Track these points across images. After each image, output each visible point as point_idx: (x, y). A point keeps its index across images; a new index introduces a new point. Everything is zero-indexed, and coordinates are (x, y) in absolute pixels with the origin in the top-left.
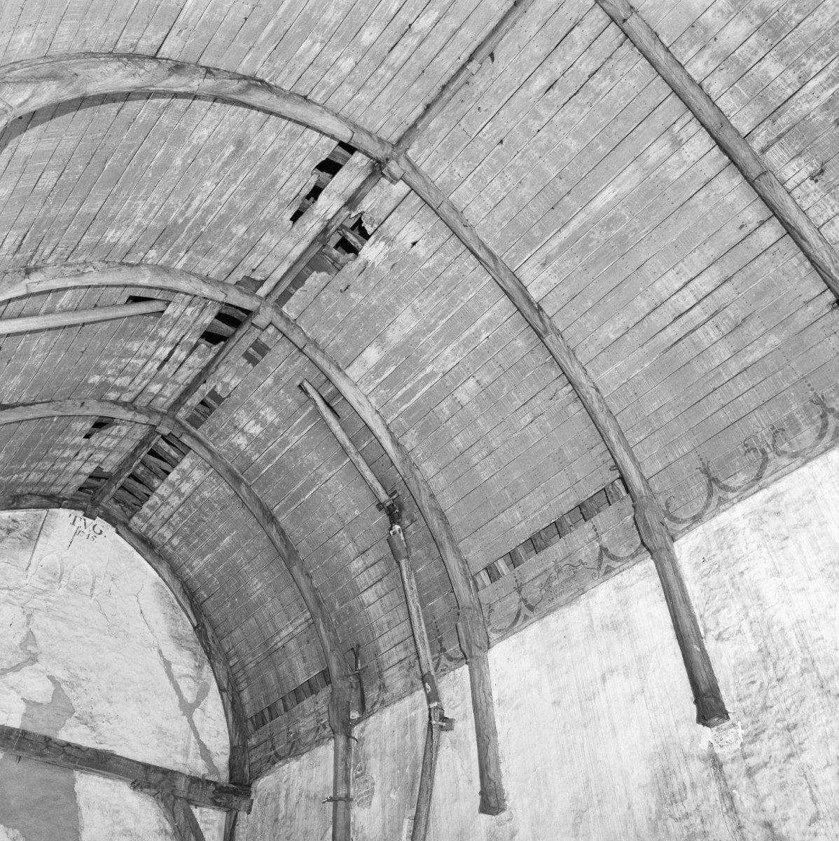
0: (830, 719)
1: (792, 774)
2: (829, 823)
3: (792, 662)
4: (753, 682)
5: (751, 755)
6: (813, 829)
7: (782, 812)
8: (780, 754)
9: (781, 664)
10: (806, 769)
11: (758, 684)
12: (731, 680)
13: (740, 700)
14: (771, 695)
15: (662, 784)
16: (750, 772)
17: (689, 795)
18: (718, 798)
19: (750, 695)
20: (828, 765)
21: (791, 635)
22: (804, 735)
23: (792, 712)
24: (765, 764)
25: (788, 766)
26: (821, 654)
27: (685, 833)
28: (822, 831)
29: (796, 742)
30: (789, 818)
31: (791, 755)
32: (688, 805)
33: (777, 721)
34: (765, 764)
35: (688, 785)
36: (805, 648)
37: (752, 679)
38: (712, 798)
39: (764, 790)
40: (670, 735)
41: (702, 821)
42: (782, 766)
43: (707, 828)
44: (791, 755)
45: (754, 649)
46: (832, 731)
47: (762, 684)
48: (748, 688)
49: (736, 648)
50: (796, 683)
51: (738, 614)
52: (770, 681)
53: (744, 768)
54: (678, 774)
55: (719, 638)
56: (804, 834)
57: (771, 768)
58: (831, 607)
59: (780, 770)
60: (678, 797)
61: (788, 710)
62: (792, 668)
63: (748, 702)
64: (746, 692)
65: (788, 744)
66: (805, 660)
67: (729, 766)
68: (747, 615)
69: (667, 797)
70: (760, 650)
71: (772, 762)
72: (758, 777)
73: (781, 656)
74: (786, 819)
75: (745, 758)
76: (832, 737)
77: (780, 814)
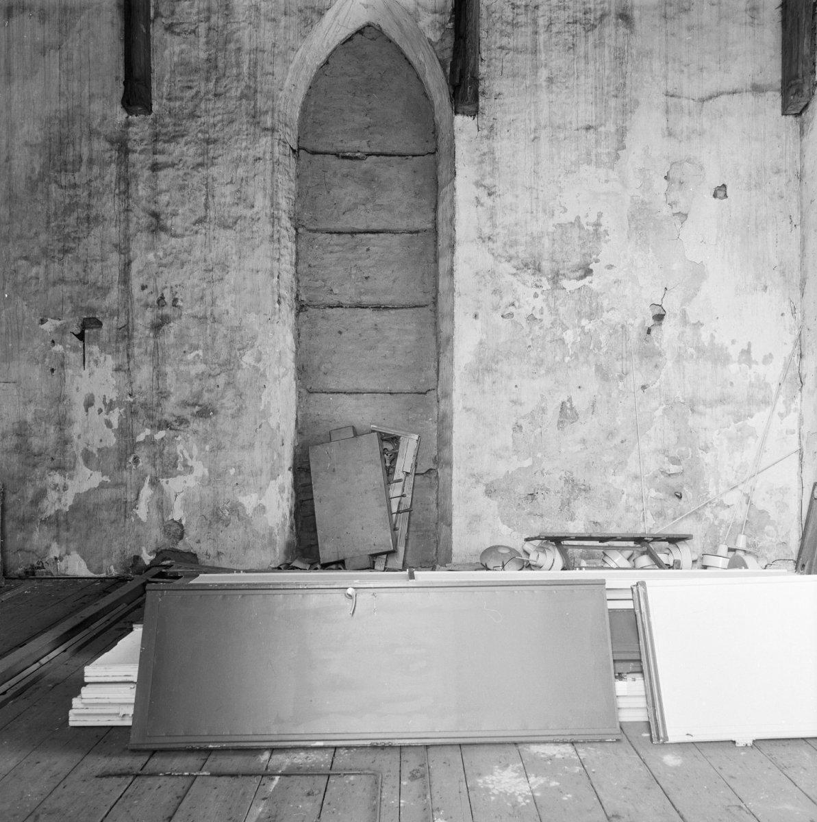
0: (249, 146)
1: (196, 179)
2: (212, 227)
3: (235, 84)
4: (190, 88)
5: (162, 152)
6: (195, 228)
7: (173, 208)
8: (191, 161)
9: (224, 82)
10: (210, 180)
11: (194, 91)
12: (167, 77)
13: (170, 99)
14: (203, 106)
15: (54, 148)
16: (155, 167)
17: (83, 169)
18: (114, 179)
19: (182, 99)
20: (231, 182)
21: (245, 58)
22: (220, 152)
23: (217, 129)
24: (173, 165)
25: (195, 173)
26: (266, 88)
27: (67, 201)
28: (204, 231)
29: (211, 155)
30: (178, 214)
31: (201, 165)
32: (79, 178)
33: (199, 131)
34: (173, 165)
35: (85, 158)
36: (253, 76)
37: (190, 84)
38: (107, 178)
39: (163, 185)
40: (79, 106)
41: (90, 195)
42: (189, 171)
43: (94, 202)
44: (201, 165)
45: (203, 55)
46: (247, 157)
47: (198, 93)
48: (182, 91)
49: (184, 46)
50: (232, 104)
51: (198, 13)
52: (207, 93)
53: (150, 161)
54: (78, 147)
55: (169, 28)
56: (186, 230)
57: (178, 169)
58: (293, 49)
59: (185, 174)
60: (70, 167)
61: (215, 125)
62: (234, 90)
63: (178, 104)
64: (178, 93)
65: (202, 154)
66: (248, 87)
67: (136, 155)
68: (208, 19)
69: (58, 164)
70: (208, 60)
71: (181, 165)
72: (161, 174)
73: (227, 74)
74: (175, 214)
75: (155, 153)
76: (245, 161)
77: (170, 209)
